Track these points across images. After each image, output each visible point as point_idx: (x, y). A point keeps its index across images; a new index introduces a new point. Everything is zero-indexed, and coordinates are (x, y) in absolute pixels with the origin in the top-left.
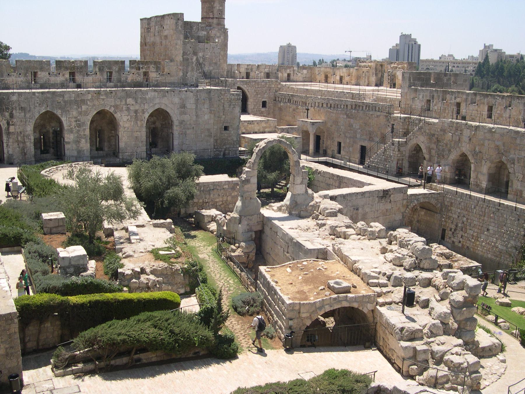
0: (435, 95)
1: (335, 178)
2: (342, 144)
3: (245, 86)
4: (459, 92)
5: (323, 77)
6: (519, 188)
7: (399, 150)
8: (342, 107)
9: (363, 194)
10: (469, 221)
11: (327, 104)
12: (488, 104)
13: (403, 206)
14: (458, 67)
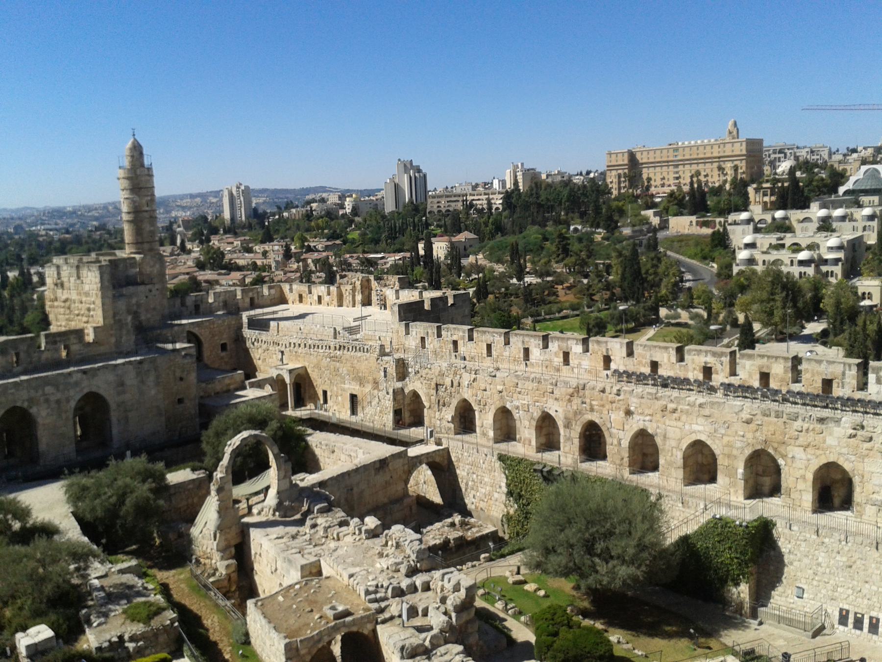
0: (430, 331)
1: (324, 447)
2: (329, 394)
3: (197, 329)
4: (455, 328)
5: (298, 299)
6: (527, 436)
7: (395, 399)
8: (324, 347)
9: (357, 470)
10: (479, 477)
11: (305, 344)
12: (486, 341)
13: (404, 472)
14: (479, 200)
